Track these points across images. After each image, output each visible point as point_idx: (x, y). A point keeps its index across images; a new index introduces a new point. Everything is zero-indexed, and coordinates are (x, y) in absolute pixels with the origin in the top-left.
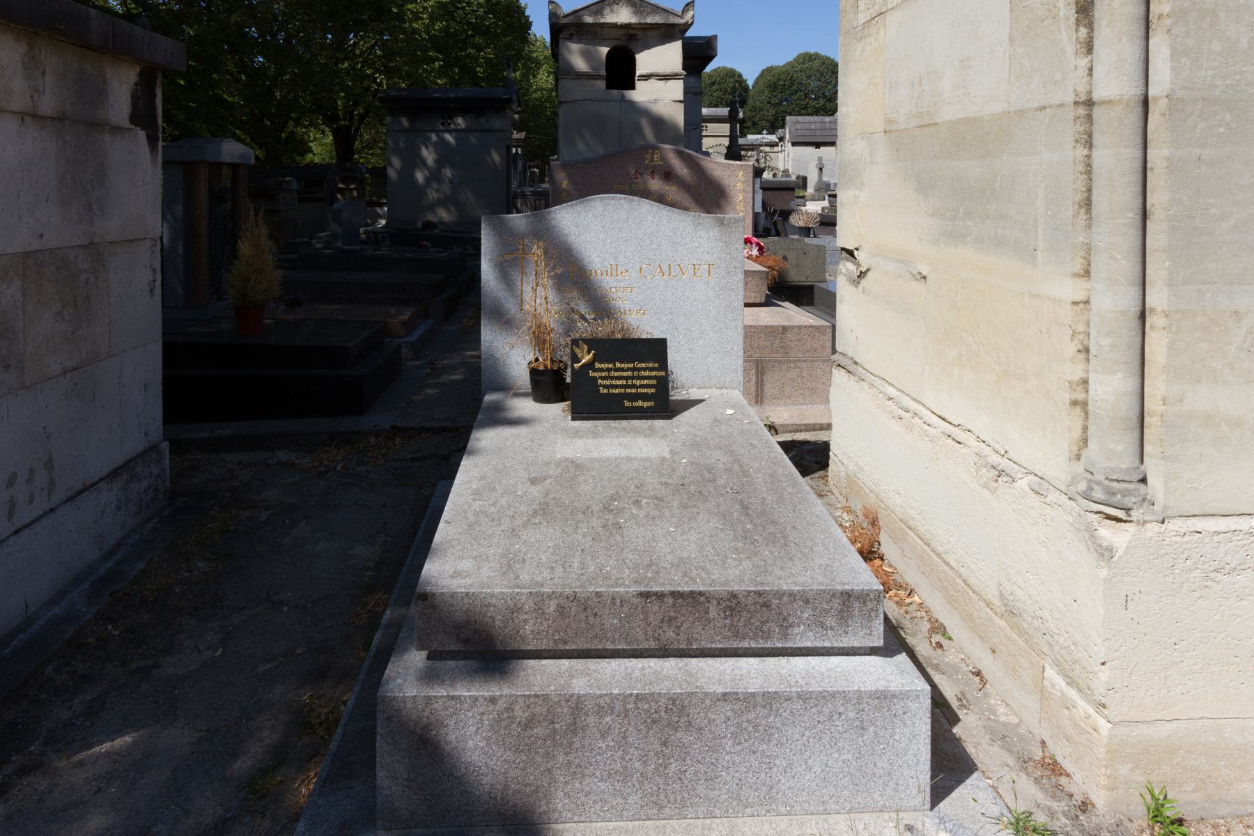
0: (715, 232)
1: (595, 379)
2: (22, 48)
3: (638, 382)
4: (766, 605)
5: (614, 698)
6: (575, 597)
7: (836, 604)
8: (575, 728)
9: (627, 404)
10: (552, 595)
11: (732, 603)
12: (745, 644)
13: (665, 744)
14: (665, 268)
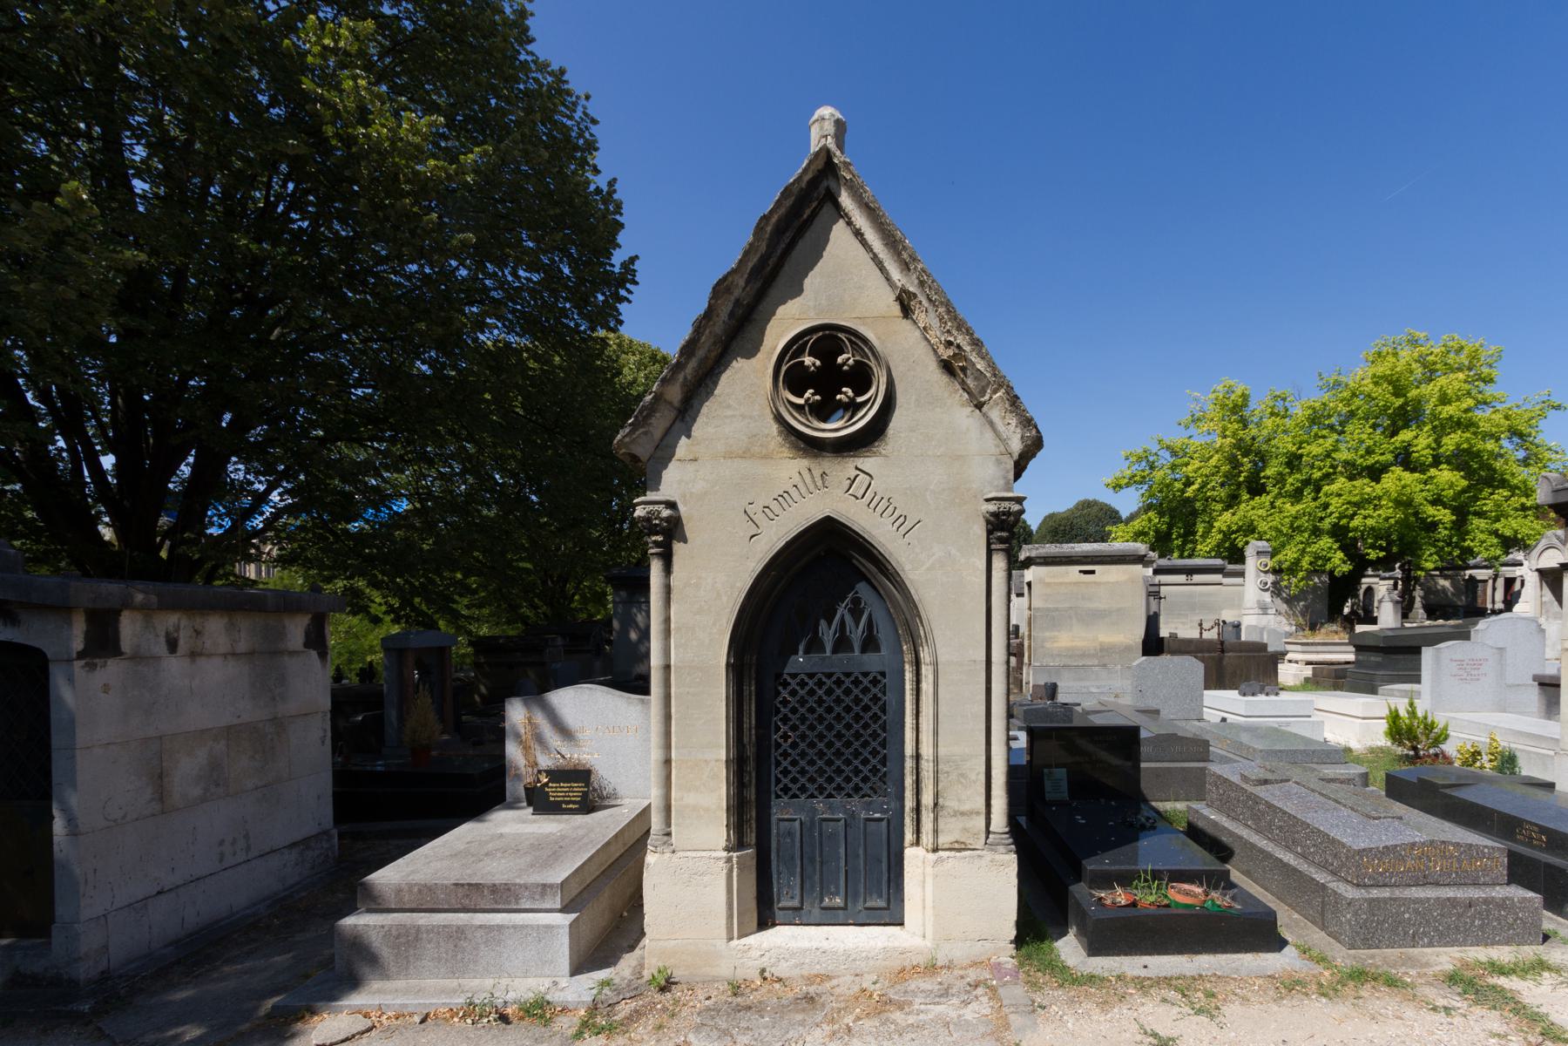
0: (639, 707)
1: (548, 792)
2: (226, 620)
3: (571, 794)
4: (509, 890)
5: (434, 926)
6: (426, 885)
7: (539, 889)
8: (417, 939)
9: (564, 806)
10: (415, 884)
11: (494, 889)
12: (499, 907)
13: (455, 946)
14: (611, 728)
